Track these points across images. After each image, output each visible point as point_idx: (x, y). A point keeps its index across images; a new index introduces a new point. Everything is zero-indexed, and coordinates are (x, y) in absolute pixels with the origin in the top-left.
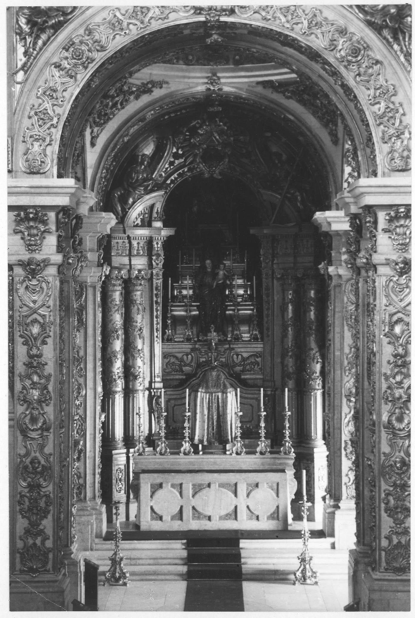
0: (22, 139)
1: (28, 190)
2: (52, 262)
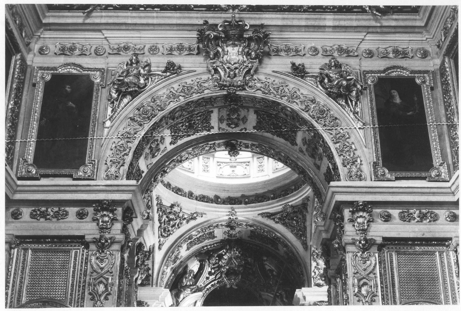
0: (105, 162)
1: (104, 188)
2: (117, 240)
